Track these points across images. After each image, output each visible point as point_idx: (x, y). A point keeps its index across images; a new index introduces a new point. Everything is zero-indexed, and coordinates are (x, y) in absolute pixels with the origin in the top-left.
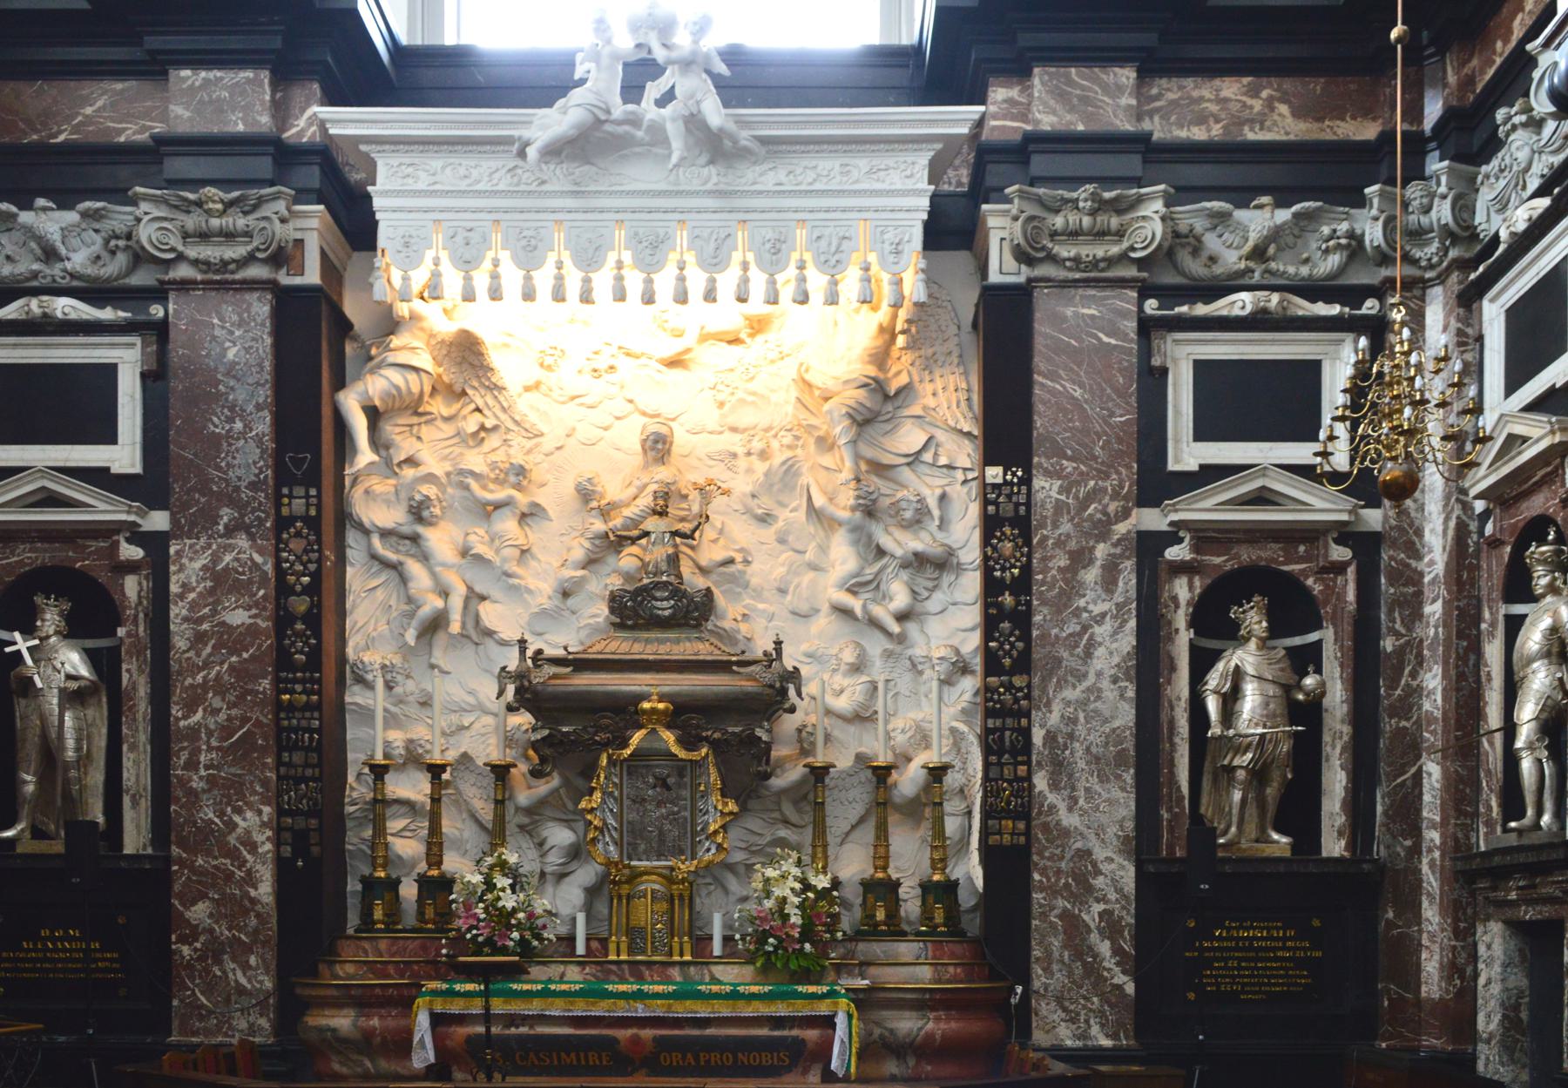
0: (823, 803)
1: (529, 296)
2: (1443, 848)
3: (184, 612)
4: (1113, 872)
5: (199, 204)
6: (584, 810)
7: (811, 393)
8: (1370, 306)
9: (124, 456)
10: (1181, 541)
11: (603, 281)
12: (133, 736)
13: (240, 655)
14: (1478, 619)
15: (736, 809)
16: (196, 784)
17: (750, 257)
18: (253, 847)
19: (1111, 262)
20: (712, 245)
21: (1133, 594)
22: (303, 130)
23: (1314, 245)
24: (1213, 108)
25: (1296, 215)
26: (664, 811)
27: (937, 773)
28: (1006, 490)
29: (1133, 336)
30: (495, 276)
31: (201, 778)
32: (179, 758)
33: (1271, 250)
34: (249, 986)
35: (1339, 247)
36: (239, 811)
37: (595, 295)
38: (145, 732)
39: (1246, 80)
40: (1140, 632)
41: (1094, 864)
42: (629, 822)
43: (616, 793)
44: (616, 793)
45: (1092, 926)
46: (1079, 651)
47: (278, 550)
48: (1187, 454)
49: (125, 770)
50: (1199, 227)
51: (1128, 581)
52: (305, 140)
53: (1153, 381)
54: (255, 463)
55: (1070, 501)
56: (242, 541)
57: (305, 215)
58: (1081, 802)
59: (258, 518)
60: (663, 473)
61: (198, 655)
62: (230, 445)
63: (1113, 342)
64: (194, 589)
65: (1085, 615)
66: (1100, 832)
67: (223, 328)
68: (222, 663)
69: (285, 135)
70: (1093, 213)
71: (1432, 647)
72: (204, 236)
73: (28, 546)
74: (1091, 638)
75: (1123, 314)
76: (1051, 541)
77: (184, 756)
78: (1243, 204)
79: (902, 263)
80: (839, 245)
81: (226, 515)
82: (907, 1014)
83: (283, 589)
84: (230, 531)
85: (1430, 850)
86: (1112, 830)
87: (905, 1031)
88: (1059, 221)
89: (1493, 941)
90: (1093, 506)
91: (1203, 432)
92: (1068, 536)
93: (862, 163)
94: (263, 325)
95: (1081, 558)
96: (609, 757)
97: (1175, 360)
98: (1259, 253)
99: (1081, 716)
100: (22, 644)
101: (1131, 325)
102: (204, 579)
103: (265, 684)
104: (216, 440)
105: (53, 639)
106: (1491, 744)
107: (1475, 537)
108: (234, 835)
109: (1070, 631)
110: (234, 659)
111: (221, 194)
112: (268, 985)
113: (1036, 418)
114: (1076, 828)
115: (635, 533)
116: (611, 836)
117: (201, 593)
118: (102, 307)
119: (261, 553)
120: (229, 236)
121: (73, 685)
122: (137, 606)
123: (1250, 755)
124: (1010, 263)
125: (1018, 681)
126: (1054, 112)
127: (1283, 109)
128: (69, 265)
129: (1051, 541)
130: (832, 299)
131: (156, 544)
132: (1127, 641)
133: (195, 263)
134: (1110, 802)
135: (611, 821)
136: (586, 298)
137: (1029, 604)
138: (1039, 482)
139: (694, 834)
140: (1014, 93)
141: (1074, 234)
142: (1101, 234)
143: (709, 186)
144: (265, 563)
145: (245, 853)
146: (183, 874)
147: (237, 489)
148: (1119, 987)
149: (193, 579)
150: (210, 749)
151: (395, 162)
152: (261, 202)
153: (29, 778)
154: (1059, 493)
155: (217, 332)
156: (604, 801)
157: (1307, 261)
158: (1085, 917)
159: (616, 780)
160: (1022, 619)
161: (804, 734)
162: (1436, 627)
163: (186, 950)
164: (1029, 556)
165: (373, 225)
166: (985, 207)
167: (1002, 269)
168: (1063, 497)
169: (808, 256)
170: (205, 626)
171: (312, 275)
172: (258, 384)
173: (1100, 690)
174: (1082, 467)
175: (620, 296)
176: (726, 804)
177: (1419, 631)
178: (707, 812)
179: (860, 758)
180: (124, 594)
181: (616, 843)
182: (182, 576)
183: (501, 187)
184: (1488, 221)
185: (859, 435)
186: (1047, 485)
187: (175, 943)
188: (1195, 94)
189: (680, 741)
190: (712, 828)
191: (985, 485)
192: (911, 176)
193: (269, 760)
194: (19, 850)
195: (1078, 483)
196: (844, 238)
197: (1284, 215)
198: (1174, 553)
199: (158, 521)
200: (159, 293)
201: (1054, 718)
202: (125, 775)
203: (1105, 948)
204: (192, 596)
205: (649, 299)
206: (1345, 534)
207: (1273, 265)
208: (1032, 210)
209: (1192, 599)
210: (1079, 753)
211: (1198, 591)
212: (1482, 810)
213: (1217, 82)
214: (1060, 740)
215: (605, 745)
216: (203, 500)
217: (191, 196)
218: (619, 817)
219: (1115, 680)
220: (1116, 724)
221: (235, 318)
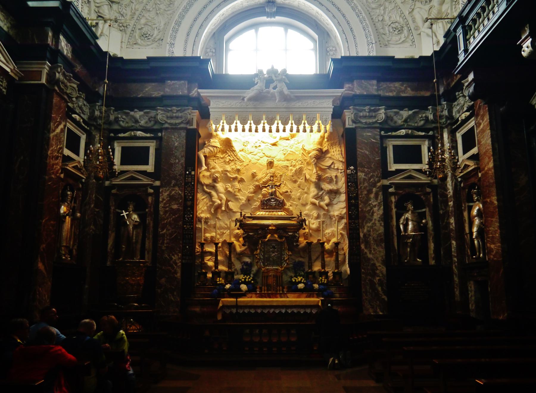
0: (311, 252)
1: (244, 130)
2: (457, 262)
3: (163, 205)
4: (381, 269)
5: (171, 111)
7: (306, 152)
8: (431, 133)
9: (150, 168)
10: (392, 187)
11: (260, 127)
13: (175, 216)
14: (462, 206)
15: (291, 254)
16: (164, 248)
17: (293, 122)
18: (176, 264)
19: (373, 123)
20: (285, 119)
21: (382, 200)
22: (194, 93)
23: (418, 119)
24: (394, 89)
25: (413, 112)
27: (337, 244)
28: (352, 175)
29: (379, 139)
30: (236, 126)
31: (165, 246)
33: (408, 120)
34: (174, 300)
35: (423, 120)
36: (173, 255)
37: (258, 131)
39: (401, 83)
40: (384, 209)
41: (376, 267)
45: (376, 283)
46: (370, 214)
47: (185, 190)
48: (393, 167)
50: (392, 116)
51: (381, 197)
52: (194, 96)
53: (384, 151)
54: (180, 170)
55: (367, 178)
56: (177, 188)
57: (194, 112)
58: (372, 251)
59: (181, 183)
60: (272, 170)
61: (165, 216)
62: (175, 165)
63: (375, 141)
64: (165, 200)
65: (371, 205)
66: (377, 259)
67: (174, 138)
68: (171, 218)
69: (190, 95)
70: (369, 112)
71: (452, 213)
72: (172, 118)
74: (373, 211)
75: (376, 135)
76: (363, 188)
77: (161, 241)
78: (402, 109)
79: (327, 123)
80: (313, 119)
81: (173, 182)
83: (186, 199)
84: (174, 186)
85: (455, 263)
86: (380, 259)
88: (361, 114)
89: (471, 286)
90: (372, 179)
91: (396, 162)
92: (367, 186)
93: (318, 101)
94: (184, 138)
95: (370, 192)
96: (261, 241)
97: (389, 145)
98: (406, 121)
99: (372, 230)
100: (125, 214)
101: (378, 137)
102: (167, 197)
103: (181, 223)
104: (172, 164)
105: (131, 212)
106: (467, 237)
107: (459, 187)
108: (172, 261)
109: (368, 209)
110: (174, 217)
111: (176, 108)
112: (179, 300)
113: (358, 158)
114: (372, 258)
115: (267, 185)
116: (261, 261)
117: (167, 201)
118: (147, 133)
119: (181, 191)
120: (177, 117)
121: (137, 223)
123: (411, 239)
124: (351, 123)
125: (356, 222)
126: (359, 90)
127: (409, 89)
128: (140, 124)
129: (363, 188)
130: (311, 131)
131: (156, 189)
132: (381, 212)
133: (169, 124)
134: (380, 251)
135: (262, 257)
136: (256, 131)
137: (358, 203)
138: (359, 174)
139: (281, 260)
140: (350, 85)
141: (365, 117)
142: (371, 117)
143: (284, 106)
144: (182, 194)
145: (174, 265)
147: (176, 176)
148: (384, 299)
149: (165, 197)
150: (167, 239)
151: (214, 101)
152: (185, 110)
153: (124, 246)
154: (364, 176)
155: (173, 139)
157: (416, 122)
158: (375, 281)
159: (263, 247)
160: (357, 206)
161: (305, 234)
162: (452, 208)
163: (159, 291)
164: (358, 191)
165: (209, 115)
166: (345, 110)
167: (349, 124)
168: (365, 177)
169: (306, 122)
170: (167, 209)
171: (194, 126)
172: (182, 151)
173: (376, 224)
174: (369, 170)
175: (264, 130)
176: (289, 253)
177: (448, 209)
178: (284, 254)
179: (319, 240)
180: (148, 201)
181: (262, 263)
182: (163, 197)
183: (238, 106)
184: (456, 115)
185: (317, 161)
186: (361, 174)
188: (390, 85)
189: (278, 237)
191: (347, 174)
192: (329, 104)
193: (181, 242)
195: (368, 174)
196: (314, 118)
197: (411, 112)
198: (391, 190)
199: (157, 183)
200: (160, 130)
201: (365, 231)
202: (146, 245)
203: (380, 289)
204: (165, 201)
205: (270, 131)
206: (429, 185)
207: (409, 123)
208: (355, 112)
209: (395, 201)
210: (372, 239)
211: (397, 199)
212: (466, 253)
213: (394, 83)
214: (367, 236)
215: (260, 238)
216: (168, 178)
217: (170, 109)
218: (264, 256)
219: (379, 221)
220: (380, 232)
221: (177, 136)
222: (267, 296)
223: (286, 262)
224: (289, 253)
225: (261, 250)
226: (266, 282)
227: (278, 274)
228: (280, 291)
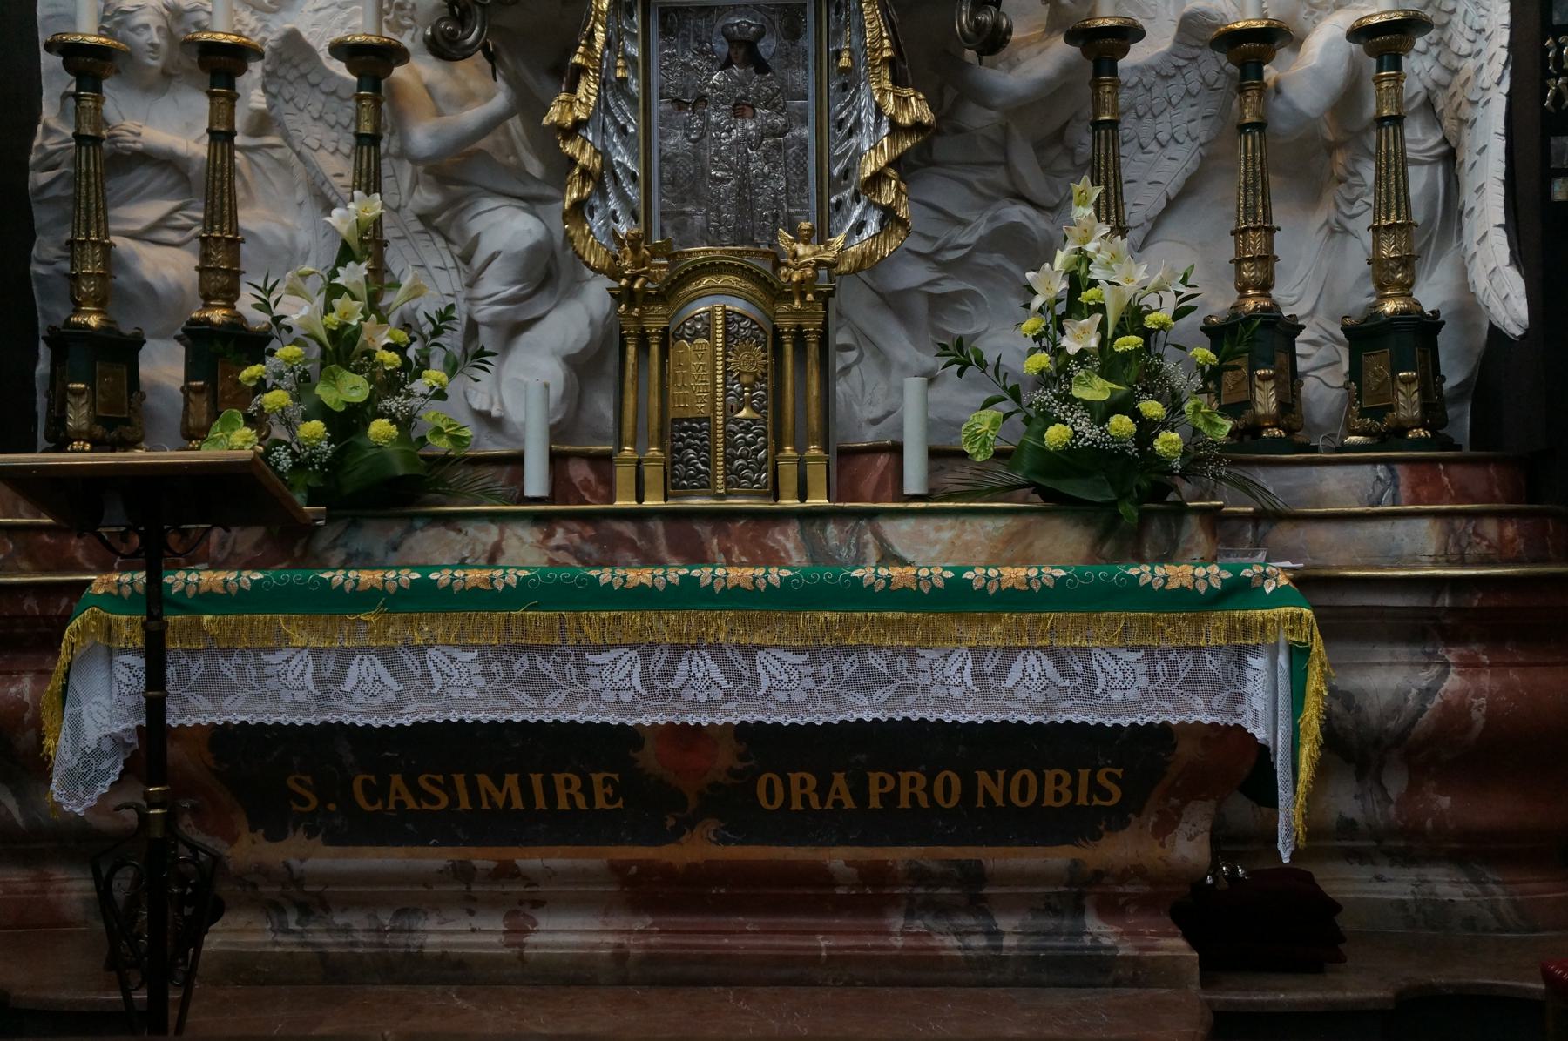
6: (558, 128)
15: (927, 116)
26: (750, 126)
42: (664, 159)
43: (635, 87)
44: (635, 87)
82: (1383, 653)
87: (1386, 698)
116: (623, 197)
135: (621, 157)
156: (603, 106)
159: (634, 50)
176: (903, 102)
190: (869, 168)
222: (664, 553)
223: (871, 204)
224: (903, 102)
225: (611, 87)
226: (655, 401)
227: (786, 315)
228: (803, 496)
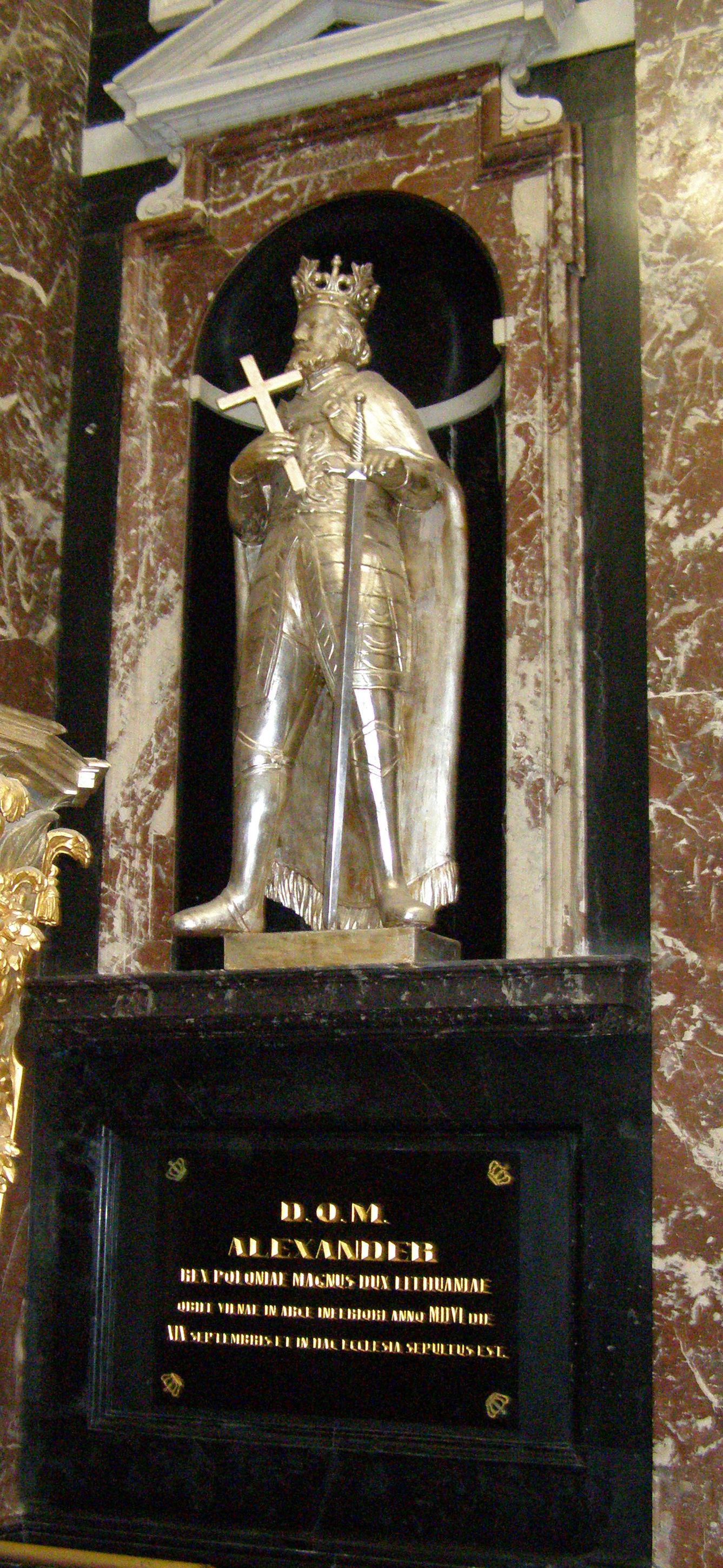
12: (535, 612)
32: (671, 652)
38: (571, 592)
49: (512, 714)
73: (283, 161)
105: (331, 374)
122: (544, 251)
146: (687, 1018)
180: (510, 231)
187: (664, 1251)
194: (233, 962)
202: (513, 727)
